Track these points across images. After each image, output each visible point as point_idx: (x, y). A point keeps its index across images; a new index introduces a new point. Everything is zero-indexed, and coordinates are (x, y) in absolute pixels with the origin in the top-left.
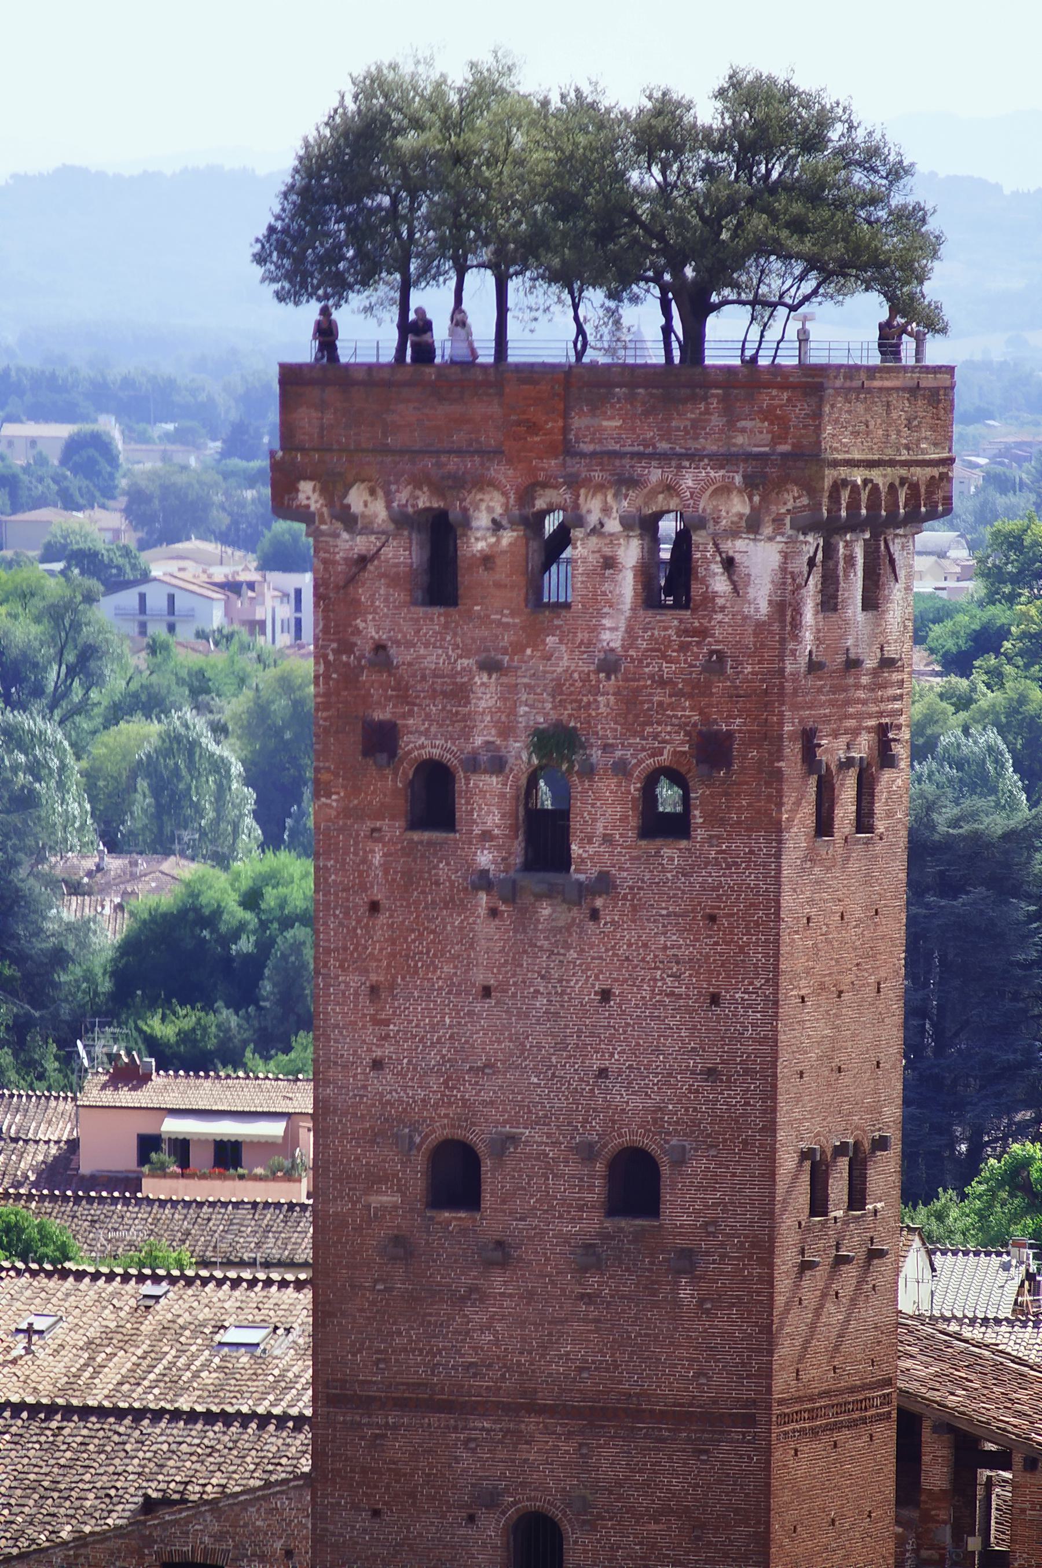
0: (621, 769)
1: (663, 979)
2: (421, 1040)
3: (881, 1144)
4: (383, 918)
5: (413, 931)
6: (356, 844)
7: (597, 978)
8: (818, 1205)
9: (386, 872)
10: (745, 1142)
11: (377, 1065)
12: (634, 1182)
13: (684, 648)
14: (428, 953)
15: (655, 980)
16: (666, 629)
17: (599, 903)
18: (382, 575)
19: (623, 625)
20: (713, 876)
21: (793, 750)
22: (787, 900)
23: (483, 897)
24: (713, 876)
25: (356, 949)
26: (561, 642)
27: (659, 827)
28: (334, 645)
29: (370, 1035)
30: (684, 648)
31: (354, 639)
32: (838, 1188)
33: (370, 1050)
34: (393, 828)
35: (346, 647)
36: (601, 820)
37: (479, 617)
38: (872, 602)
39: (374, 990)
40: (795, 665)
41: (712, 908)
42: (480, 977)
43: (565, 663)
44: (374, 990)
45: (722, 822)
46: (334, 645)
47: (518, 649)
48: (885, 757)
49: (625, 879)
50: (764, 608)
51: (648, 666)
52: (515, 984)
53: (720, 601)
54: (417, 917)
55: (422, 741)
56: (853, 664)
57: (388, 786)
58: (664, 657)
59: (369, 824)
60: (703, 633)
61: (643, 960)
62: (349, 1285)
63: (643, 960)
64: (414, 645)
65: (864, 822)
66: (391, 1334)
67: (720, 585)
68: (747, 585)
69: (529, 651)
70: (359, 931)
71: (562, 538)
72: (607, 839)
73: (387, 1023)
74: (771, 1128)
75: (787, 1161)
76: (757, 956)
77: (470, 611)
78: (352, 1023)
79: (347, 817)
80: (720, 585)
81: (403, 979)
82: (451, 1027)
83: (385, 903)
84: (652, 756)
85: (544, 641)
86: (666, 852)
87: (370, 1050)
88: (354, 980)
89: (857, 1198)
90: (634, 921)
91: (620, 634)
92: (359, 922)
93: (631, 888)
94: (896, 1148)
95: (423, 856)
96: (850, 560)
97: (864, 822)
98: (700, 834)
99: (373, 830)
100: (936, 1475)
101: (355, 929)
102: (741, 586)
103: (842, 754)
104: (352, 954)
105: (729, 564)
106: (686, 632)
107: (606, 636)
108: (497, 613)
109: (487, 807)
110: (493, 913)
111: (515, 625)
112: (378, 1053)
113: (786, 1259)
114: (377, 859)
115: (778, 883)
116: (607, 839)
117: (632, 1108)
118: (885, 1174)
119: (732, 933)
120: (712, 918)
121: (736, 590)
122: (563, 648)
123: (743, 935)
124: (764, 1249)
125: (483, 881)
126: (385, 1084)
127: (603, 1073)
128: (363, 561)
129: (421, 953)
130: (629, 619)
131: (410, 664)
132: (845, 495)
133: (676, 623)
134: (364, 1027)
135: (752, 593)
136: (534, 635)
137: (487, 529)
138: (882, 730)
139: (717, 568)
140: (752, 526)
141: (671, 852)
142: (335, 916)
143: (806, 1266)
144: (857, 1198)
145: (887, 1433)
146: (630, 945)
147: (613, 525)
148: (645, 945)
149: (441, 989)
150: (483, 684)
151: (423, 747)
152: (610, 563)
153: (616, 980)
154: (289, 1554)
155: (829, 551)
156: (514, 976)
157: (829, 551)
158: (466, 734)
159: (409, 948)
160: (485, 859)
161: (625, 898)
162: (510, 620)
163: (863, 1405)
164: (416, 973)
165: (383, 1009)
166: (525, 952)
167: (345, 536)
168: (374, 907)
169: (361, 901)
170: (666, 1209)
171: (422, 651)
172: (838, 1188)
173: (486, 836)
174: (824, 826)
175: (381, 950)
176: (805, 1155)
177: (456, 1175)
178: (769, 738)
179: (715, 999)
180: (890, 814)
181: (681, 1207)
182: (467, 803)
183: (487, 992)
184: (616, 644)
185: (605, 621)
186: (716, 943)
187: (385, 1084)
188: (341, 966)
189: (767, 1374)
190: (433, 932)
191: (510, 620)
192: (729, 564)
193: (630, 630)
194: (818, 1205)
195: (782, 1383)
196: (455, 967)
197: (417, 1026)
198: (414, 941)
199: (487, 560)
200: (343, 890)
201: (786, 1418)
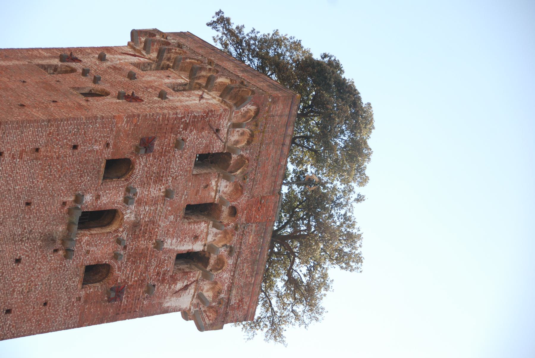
0: (116, 256)
1: (22, 286)
2: (9, 175)
4: (70, 152)
5: (62, 167)
6: (104, 137)
7: (28, 256)
9: (90, 152)
13: (158, 274)
14: (50, 175)
15: (21, 283)
16: (167, 265)
17: (61, 252)
18: (210, 140)
19: (172, 247)
20: (63, 302)
23: (72, 199)
24: (63, 302)
25: (57, 140)
26: (171, 222)
28: (188, 121)
29: (16, 149)
31: (188, 130)
33: (8, 150)
34: (108, 154)
37: (186, 185)
39: (37, 150)
41: (50, 304)
43: (162, 224)
44: (37, 150)
45: (86, 302)
46: (188, 121)
49: (70, 263)
50: (166, 305)
51: (155, 260)
52: (30, 218)
53: (173, 287)
54: (68, 168)
55: (142, 165)
57: (126, 148)
58: (156, 267)
59: (111, 142)
60: (163, 281)
61: (32, 276)
63: (32, 276)
64: (181, 157)
67: (179, 285)
68: (177, 297)
69: (170, 208)
70: (65, 141)
72: (88, 252)
73: (21, 158)
77: (190, 181)
78: (23, 140)
79: (117, 132)
80: (179, 285)
81: (40, 164)
82: (14, 189)
83: (76, 152)
84: (119, 268)
85: (172, 214)
87: (8, 150)
88: (43, 141)
90: (50, 270)
92: (69, 140)
93: (65, 266)
95: (94, 169)
99: (108, 145)
101: (66, 139)
102: (177, 294)
104: (55, 138)
105: (186, 287)
108: (187, 193)
109: (111, 197)
110: (64, 203)
111: (181, 201)
114: (96, 147)
116: (88, 252)
119: (38, 314)
120: (45, 304)
121: (176, 292)
122: (168, 223)
125: (78, 199)
128: (218, 130)
129: (51, 172)
130: (174, 249)
131: (174, 156)
133: (168, 269)
134: (20, 146)
135: (174, 299)
137: (220, 188)
139: (185, 284)
140: (200, 297)
142: (74, 129)
146: (40, 269)
147: (210, 239)
148: (38, 276)
149: (33, 182)
150: (160, 189)
151: (140, 164)
152: (196, 238)
153: (25, 265)
156: (34, 217)
158: (142, 184)
159: (54, 165)
160: (88, 198)
161: (61, 264)
162: (183, 198)
164: (42, 170)
165: (27, 155)
166: (44, 221)
167: (229, 124)
169: (79, 141)
171: (178, 161)
173: (98, 197)
175: (55, 152)
179: (8, 311)
182: (113, 187)
184: (165, 246)
185: (175, 240)
186: (34, 308)
188: (50, 133)
190: (60, 177)
191: (183, 198)
192: (186, 287)
193: (170, 251)
196: (42, 189)
197: (17, 173)
198: (57, 168)
200: (85, 132)
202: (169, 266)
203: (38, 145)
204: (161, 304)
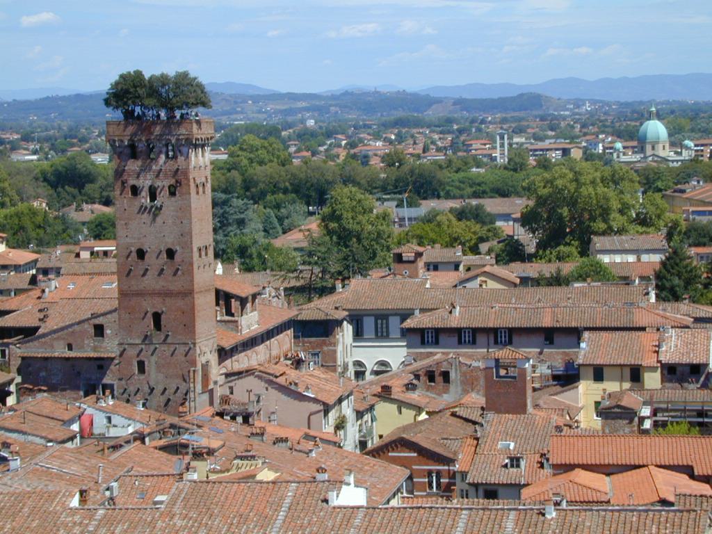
8: (200, 256)
12: (171, 254)
21: (192, 181)
22: (193, 206)
27: (172, 194)
32: (203, 253)
38: (203, 156)
40: (192, 167)
42: (143, 221)
48: (207, 182)
55: (132, 182)
62: (125, 274)
65: (204, 192)
71: (153, 147)
75: (195, 249)
89: (206, 254)
97: (204, 192)
109: (145, 193)
113: (195, 266)
117: (170, 241)
123: (185, 212)
124: (191, 264)
126: (128, 240)
141: (173, 199)
144: (206, 254)
145: (214, 294)
160: (143, 201)
163: (210, 290)
172: (203, 253)
174: (198, 193)
181: (177, 257)
187: (128, 240)
189: (193, 285)
194: (200, 256)
195: (196, 286)
199: (141, 152)
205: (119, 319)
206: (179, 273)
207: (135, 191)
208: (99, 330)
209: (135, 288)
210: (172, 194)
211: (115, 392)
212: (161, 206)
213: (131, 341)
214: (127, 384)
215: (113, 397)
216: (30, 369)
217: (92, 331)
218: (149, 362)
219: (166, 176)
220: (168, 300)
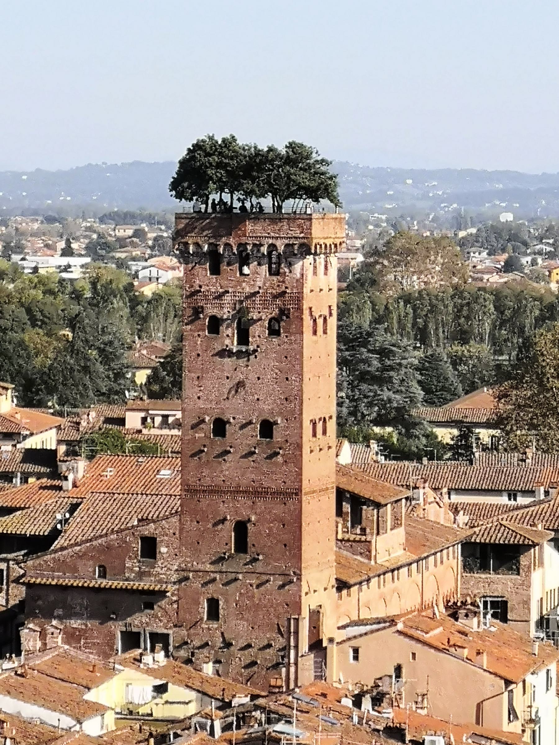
3: (331, 417)
4: (200, 358)
8: (314, 435)
10: (295, 418)
11: (199, 398)
12: (267, 429)
20: (286, 346)
24: (286, 346)
30: (278, 286)
35: (192, 286)
36: (258, 332)
38: (326, 274)
40: (306, 291)
44: (198, 377)
47: (236, 286)
48: (331, 315)
50: (299, 276)
55: (211, 310)
56: (321, 290)
60: (283, 282)
65: (325, 332)
66: (202, 473)
74: (301, 414)
76: (297, 367)
80: (287, 270)
86: (274, 340)
88: (193, 375)
89: (324, 432)
91: (262, 283)
94: (334, 419)
96: (320, 263)
97: (325, 332)
98: (282, 335)
100: (347, 507)
103: (319, 314)
106: (279, 282)
107: (258, 283)
112: (199, 395)
115: (302, 348)
118: (332, 426)
121: (290, 272)
124: (299, 447)
127: (258, 399)
132: (318, 247)
136: (239, 283)
138: (330, 307)
141: (275, 340)
143: (311, 451)
144: (324, 432)
145: (333, 496)
154: (174, 534)
155: (315, 260)
157: (315, 260)
160: (227, 342)
163: (327, 489)
168: (198, 355)
170: (274, 437)
174: (315, 333)
176: (311, 421)
177: (220, 426)
178: (300, 309)
179: (287, 379)
180: (331, 329)
181: (278, 436)
183: (228, 378)
187: (201, 404)
194: (314, 435)
201: (306, 494)
202: (275, 278)
203: (195, 378)
204: (297, 280)
205: (181, 530)
206: (280, 459)
207: (215, 325)
208: (149, 547)
209: (207, 481)
210: (274, 332)
211: (171, 648)
212: (255, 351)
213: (200, 567)
214: (188, 635)
215: (167, 656)
216: (40, 602)
217: (138, 546)
218: (226, 601)
219: (265, 304)
220: (260, 503)
